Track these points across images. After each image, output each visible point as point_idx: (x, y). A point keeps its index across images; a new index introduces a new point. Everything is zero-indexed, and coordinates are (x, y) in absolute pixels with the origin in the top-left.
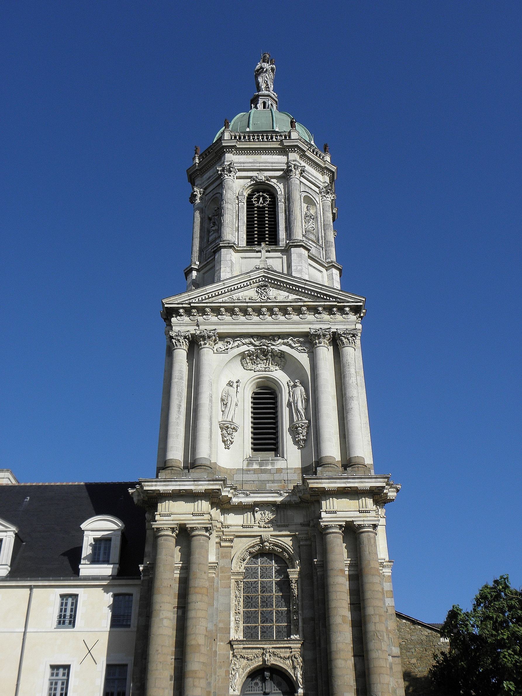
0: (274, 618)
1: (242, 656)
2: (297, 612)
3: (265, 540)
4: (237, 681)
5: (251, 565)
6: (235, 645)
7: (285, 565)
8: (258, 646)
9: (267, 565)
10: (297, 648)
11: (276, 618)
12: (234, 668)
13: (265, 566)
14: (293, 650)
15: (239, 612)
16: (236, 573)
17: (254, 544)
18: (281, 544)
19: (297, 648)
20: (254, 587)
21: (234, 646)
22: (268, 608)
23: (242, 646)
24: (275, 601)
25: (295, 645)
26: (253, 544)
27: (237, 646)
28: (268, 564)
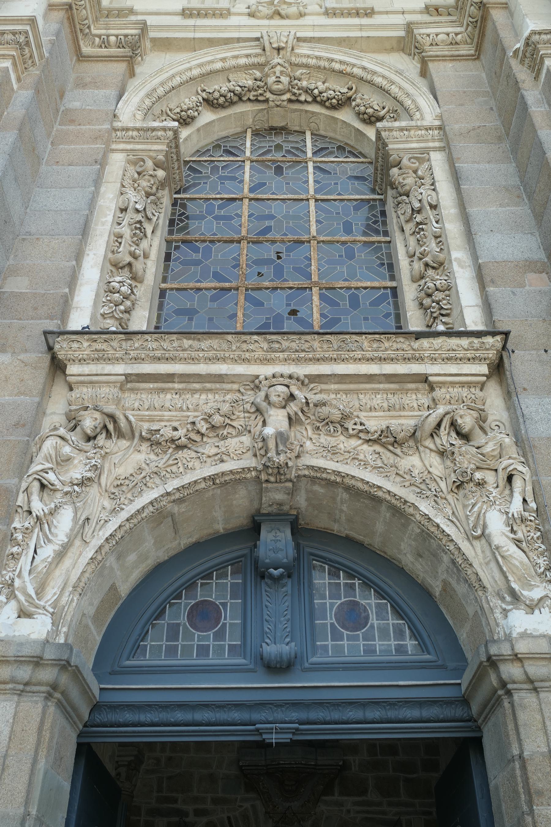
0: (316, 315)
1: (112, 417)
2: (441, 264)
3: (275, 45)
4: (60, 555)
5: (211, 156)
6: (82, 361)
7: (362, 160)
8: (222, 368)
9: (281, 159)
10: (462, 385)
11: (322, 315)
12: (51, 476)
13: (274, 162)
14: (439, 393)
15: (130, 265)
16: (135, 133)
17: (227, 65)
18: (341, 62)
19: (462, 385)
20: (217, 218)
21: (72, 369)
22: (286, 280)
23: (120, 368)
24: (319, 260)
25: (453, 369)
26: (219, 65)
27: (86, 369)
28: (284, 156)
